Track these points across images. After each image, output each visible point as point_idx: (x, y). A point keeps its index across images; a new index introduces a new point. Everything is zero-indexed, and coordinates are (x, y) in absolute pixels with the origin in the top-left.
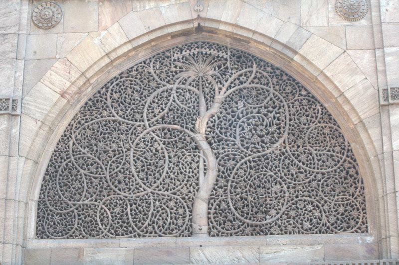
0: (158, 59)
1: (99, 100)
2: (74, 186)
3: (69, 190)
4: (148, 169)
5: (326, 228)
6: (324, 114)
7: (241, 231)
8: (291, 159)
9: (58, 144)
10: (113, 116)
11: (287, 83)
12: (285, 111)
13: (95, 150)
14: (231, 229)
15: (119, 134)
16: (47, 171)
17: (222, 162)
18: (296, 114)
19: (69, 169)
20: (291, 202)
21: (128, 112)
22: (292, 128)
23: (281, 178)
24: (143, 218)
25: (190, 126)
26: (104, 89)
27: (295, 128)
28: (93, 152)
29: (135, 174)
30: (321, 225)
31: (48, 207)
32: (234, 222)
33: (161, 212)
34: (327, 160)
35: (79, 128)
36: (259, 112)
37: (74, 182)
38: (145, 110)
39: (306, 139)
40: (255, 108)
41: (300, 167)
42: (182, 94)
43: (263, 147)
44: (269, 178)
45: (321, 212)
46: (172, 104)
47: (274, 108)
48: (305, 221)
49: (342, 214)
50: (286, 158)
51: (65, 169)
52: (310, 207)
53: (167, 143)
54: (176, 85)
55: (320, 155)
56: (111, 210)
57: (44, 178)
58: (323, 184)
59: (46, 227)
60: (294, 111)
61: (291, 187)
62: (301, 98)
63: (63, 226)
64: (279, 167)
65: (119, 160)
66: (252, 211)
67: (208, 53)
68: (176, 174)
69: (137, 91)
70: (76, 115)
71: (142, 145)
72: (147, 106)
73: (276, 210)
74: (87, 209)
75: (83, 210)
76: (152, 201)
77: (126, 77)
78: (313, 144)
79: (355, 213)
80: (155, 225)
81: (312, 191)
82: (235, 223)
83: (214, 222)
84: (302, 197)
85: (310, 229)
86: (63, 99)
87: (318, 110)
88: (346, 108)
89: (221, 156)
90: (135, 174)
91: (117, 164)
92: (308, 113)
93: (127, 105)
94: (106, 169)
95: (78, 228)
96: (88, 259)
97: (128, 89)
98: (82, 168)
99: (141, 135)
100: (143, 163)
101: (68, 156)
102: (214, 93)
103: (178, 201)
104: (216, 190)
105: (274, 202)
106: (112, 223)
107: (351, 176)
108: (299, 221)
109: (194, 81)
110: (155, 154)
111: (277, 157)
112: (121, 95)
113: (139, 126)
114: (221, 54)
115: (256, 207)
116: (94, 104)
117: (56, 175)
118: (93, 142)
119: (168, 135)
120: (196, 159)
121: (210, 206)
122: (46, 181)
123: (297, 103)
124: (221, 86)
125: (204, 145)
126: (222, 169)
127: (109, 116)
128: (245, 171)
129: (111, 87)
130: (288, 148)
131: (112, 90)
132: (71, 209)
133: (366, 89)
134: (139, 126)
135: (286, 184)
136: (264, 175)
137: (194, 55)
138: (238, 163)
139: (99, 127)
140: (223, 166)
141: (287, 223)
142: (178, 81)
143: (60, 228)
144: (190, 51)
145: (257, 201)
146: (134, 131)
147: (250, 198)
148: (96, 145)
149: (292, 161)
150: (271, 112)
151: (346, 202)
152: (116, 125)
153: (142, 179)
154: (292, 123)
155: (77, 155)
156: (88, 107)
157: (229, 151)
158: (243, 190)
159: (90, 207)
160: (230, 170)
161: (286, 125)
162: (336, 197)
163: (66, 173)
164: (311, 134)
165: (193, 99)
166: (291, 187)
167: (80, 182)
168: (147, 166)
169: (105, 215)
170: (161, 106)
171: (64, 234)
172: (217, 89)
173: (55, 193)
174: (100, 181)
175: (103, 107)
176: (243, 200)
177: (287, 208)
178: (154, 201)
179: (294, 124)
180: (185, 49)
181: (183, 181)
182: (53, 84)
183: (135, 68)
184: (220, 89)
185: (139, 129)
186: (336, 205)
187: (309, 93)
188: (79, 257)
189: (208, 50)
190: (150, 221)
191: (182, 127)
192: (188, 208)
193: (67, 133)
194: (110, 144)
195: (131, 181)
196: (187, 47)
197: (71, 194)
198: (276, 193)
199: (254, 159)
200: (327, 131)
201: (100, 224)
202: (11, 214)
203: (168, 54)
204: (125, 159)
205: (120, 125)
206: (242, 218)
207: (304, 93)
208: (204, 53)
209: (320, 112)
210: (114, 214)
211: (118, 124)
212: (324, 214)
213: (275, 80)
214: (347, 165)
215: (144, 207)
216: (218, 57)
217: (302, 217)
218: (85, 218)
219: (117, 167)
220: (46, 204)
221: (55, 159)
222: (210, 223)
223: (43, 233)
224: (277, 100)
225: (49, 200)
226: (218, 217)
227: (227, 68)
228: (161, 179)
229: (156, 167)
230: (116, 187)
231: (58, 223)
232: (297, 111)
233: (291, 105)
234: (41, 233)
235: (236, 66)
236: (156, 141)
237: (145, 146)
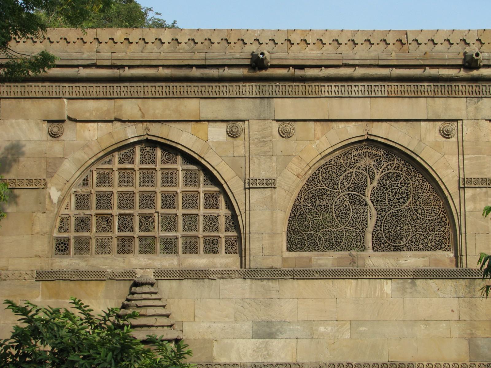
4: (342, 216)
10: (323, 186)
16: (290, 215)
17: (379, 213)
22: (414, 195)
23: (408, 221)
25: (362, 192)
26: (318, 171)
29: (336, 218)
36: (397, 186)
38: (339, 184)
39: (421, 201)
40: (395, 184)
43: (399, 205)
47: (405, 184)
49: (438, 241)
50: (411, 211)
51: (300, 215)
52: (422, 237)
54: (355, 170)
57: (289, 220)
65: (327, 210)
69: (335, 173)
76: (345, 232)
79: (444, 241)
82: (386, 245)
86: (298, 178)
89: (378, 209)
90: (336, 218)
96: (314, 263)
98: (308, 214)
99: (338, 197)
104: (376, 227)
105: (405, 234)
107: (443, 221)
109: (364, 168)
113: (337, 192)
116: (313, 180)
118: (313, 200)
119: (351, 198)
120: (366, 211)
123: (417, 182)
124: (378, 171)
125: (370, 203)
126: (379, 216)
128: (391, 218)
129: (321, 170)
130: (412, 206)
131: (322, 172)
133: (453, 177)
134: (337, 192)
136: (400, 220)
137: (364, 153)
140: (379, 215)
142: (356, 168)
143: (299, 246)
147: (393, 232)
148: (315, 202)
150: (404, 186)
153: (338, 221)
154: (414, 192)
162: (435, 232)
163: (300, 217)
165: (364, 178)
182: (293, 170)
183: (333, 160)
184: (378, 172)
185: (337, 194)
188: (310, 262)
189: (371, 150)
198: (406, 230)
200: (431, 197)
203: (350, 152)
206: (389, 242)
212: (429, 241)
213: (406, 168)
214: (441, 215)
216: (376, 155)
217: (418, 242)
223: (290, 248)
229: (346, 214)
230: (326, 224)
234: (289, 249)
236: (345, 200)
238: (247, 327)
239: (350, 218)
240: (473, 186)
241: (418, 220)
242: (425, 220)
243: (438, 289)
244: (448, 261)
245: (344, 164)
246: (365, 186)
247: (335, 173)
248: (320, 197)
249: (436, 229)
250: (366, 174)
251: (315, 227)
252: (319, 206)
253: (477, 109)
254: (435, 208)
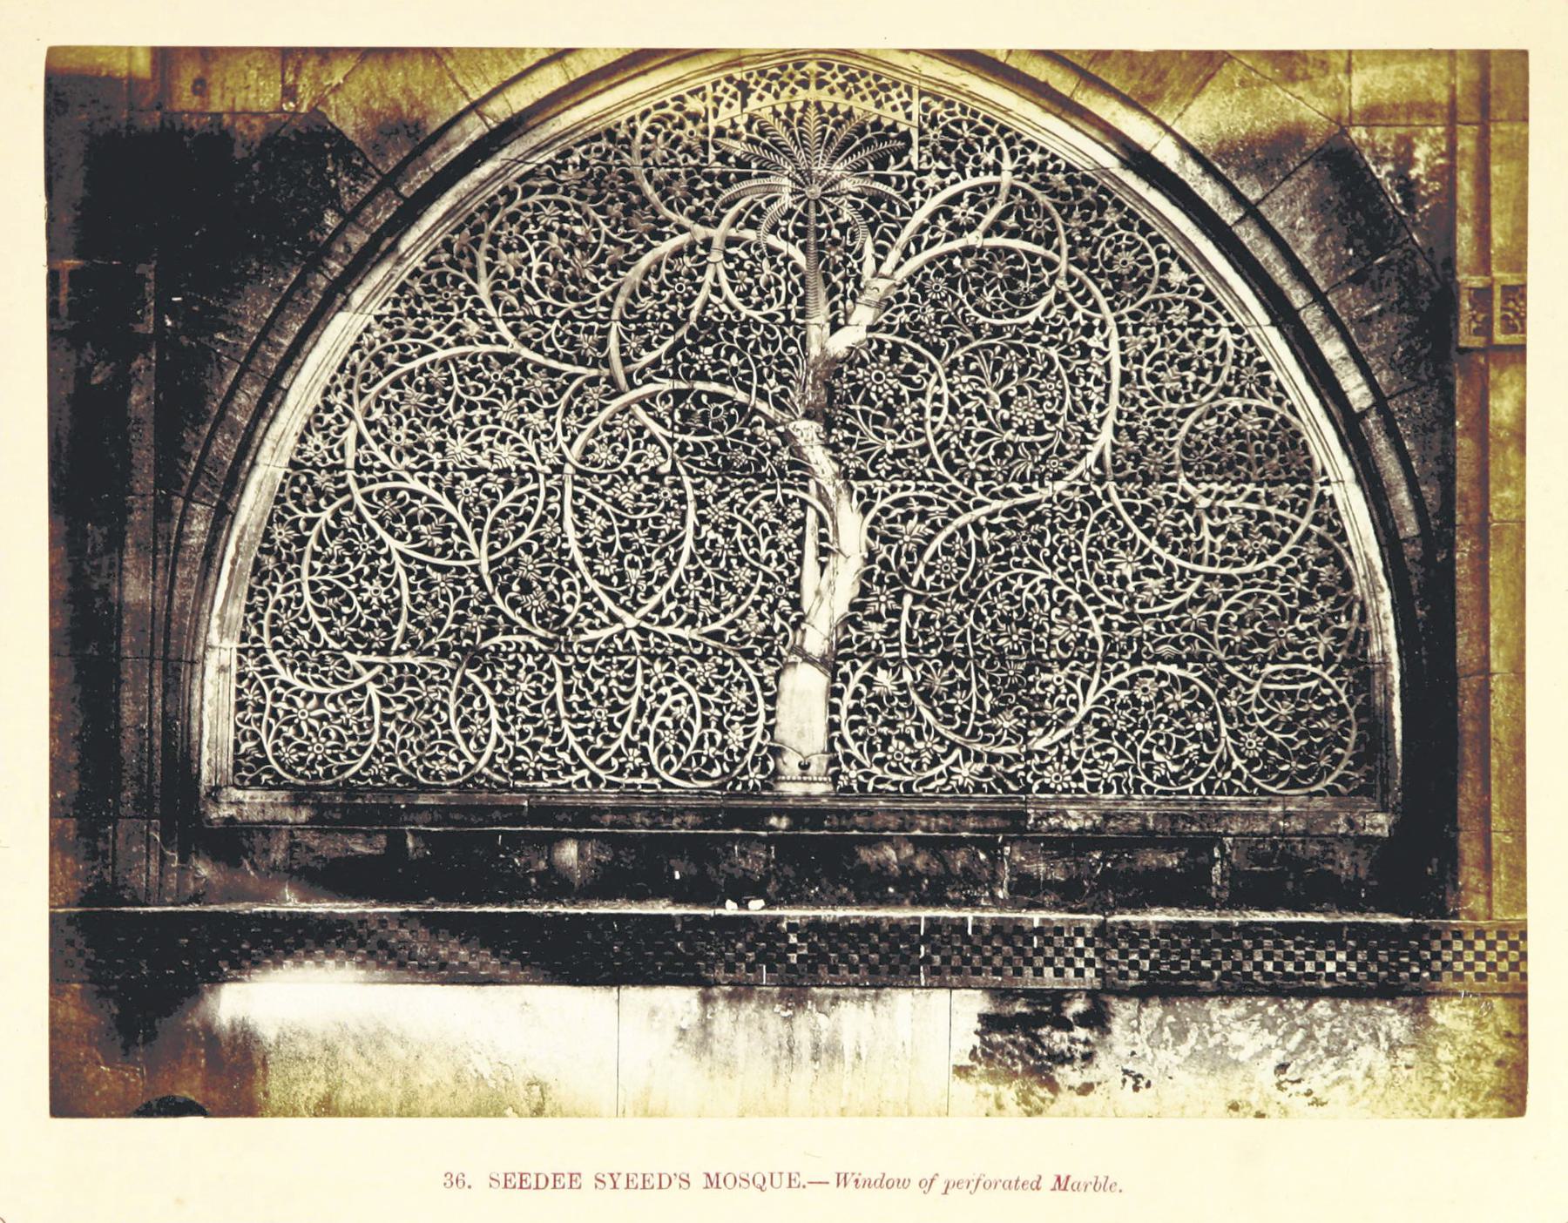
0: (658, 126)
1: (449, 279)
2: (365, 596)
3: (346, 610)
5: (1228, 775)
6: (1243, 363)
7: (941, 775)
8: (1119, 522)
9: (302, 440)
10: (501, 340)
11: (1119, 238)
12: (1106, 342)
13: (437, 466)
14: (908, 766)
15: (521, 410)
16: (267, 536)
17: (882, 529)
18: (1147, 359)
19: (347, 535)
20: (1114, 680)
21: (552, 327)
23: (1085, 590)
24: (610, 720)
27: (1141, 410)
28: (431, 475)
29: (580, 560)
30: (1213, 763)
31: (273, 671)
32: (919, 745)
33: (670, 699)
34: (1246, 528)
35: (378, 379)
37: (365, 584)
38: (616, 326)
39: (1176, 450)
41: (1152, 552)
42: (746, 265)
44: (1041, 588)
45: (1213, 716)
46: (709, 301)
48: (1160, 750)
50: (1102, 518)
51: (333, 534)
52: (1179, 700)
53: (690, 449)
56: (499, 688)
57: (258, 564)
58: (1225, 619)
59: (268, 747)
60: (1139, 347)
61: (1115, 625)
62: (1166, 295)
63: (329, 744)
64: (1079, 553)
66: (981, 705)
67: (842, 109)
68: (723, 564)
69: (583, 247)
70: (368, 330)
71: (604, 455)
72: (620, 301)
73: (1062, 704)
74: (413, 682)
75: (399, 683)
77: (545, 190)
78: (1198, 473)
80: (650, 745)
81: (1189, 640)
83: (850, 741)
84: (1153, 662)
85: (1175, 776)
87: (1224, 346)
89: (880, 504)
90: (580, 560)
91: (517, 520)
92: (1187, 355)
93: (548, 299)
94: (478, 537)
95: (382, 749)
97: (553, 235)
98: (391, 531)
99: (601, 417)
100: (609, 519)
101: (341, 486)
102: (860, 265)
103: (730, 663)
104: (859, 626)
106: (502, 734)
108: (1140, 748)
109: (790, 213)
111: (1071, 515)
112: (528, 260)
115: (996, 693)
117: (301, 555)
118: (431, 435)
121: (839, 685)
122: (265, 575)
127: (486, 340)
128: (963, 562)
130: (1111, 486)
131: (494, 239)
132: (357, 682)
134: (593, 382)
135: (1098, 613)
136: (1027, 578)
138: (938, 529)
139: (450, 381)
140: (884, 540)
141: (1097, 755)
142: (731, 213)
144: (777, 95)
145: (1000, 671)
146: (577, 402)
148: (440, 447)
149: (1123, 533)
151: (1303, 686)
152: (511, 374)
155: (372, 481)
156: (407, 301)
157: (906, 488)
158: (952, 629)
159: (423, 674)
160: (909, 556)
161: (1107, 399)
163: (335, 547)
164: (1193, 436)
166: (1115, 625)
167: (385, 582)
168: (622, 530)
169: (477, 703)
170: (672, 307)
171: (334, 772)
173: (296, 621)
174: (457, 582)
175: (461, 303)
176: (952, 666)
177: (1101, 701)
178: (647, 661)
179: (1137, 395)
180: (759, 90)
181: (747, 590)
186: (1265, 693)
187: (1197, 280)
189: (839, 97)
190: (634, 731)
191: (747, 389)
192: (764, 688)
193: (331, 398)
194: (490, 444)
195: (564, 583)
196: (764, 82)
197: (356, 624)
199: (995, 521)
201: (459, 738)
203: (693, 105)
204: (546, 504)
205: (525, 374)
207: (1177, 276)
208: (827, 107)
209: (1231, 355)
210: (507, 704)
211: (518, 373)
212: (1224, 726)
215: (613, 683)
216: (877, 125)
218: (407, 713)
219: (518, 532)
220: (265, 661)
221: (293, 496)
222: (837, 746)
224: (1082, 300)
225: (276, 646)
226: (863, 723)
228: (671, 584)
229: (654, 535)
230: (514, 604)
231: (311, 728)
232: (1150, 347)
233: (1127, 320)
235: (941, 165)
236: (652, 440)
237: (615, 459)
241: (1150, 582)
242: (1198, 581)
245: (649, 189)
246: (789, 343)
247: (583, 246)
248: (478, 413)
249: (1273, 646)
250: (800, 259)
251: (439, 623)
252: (472, 474)
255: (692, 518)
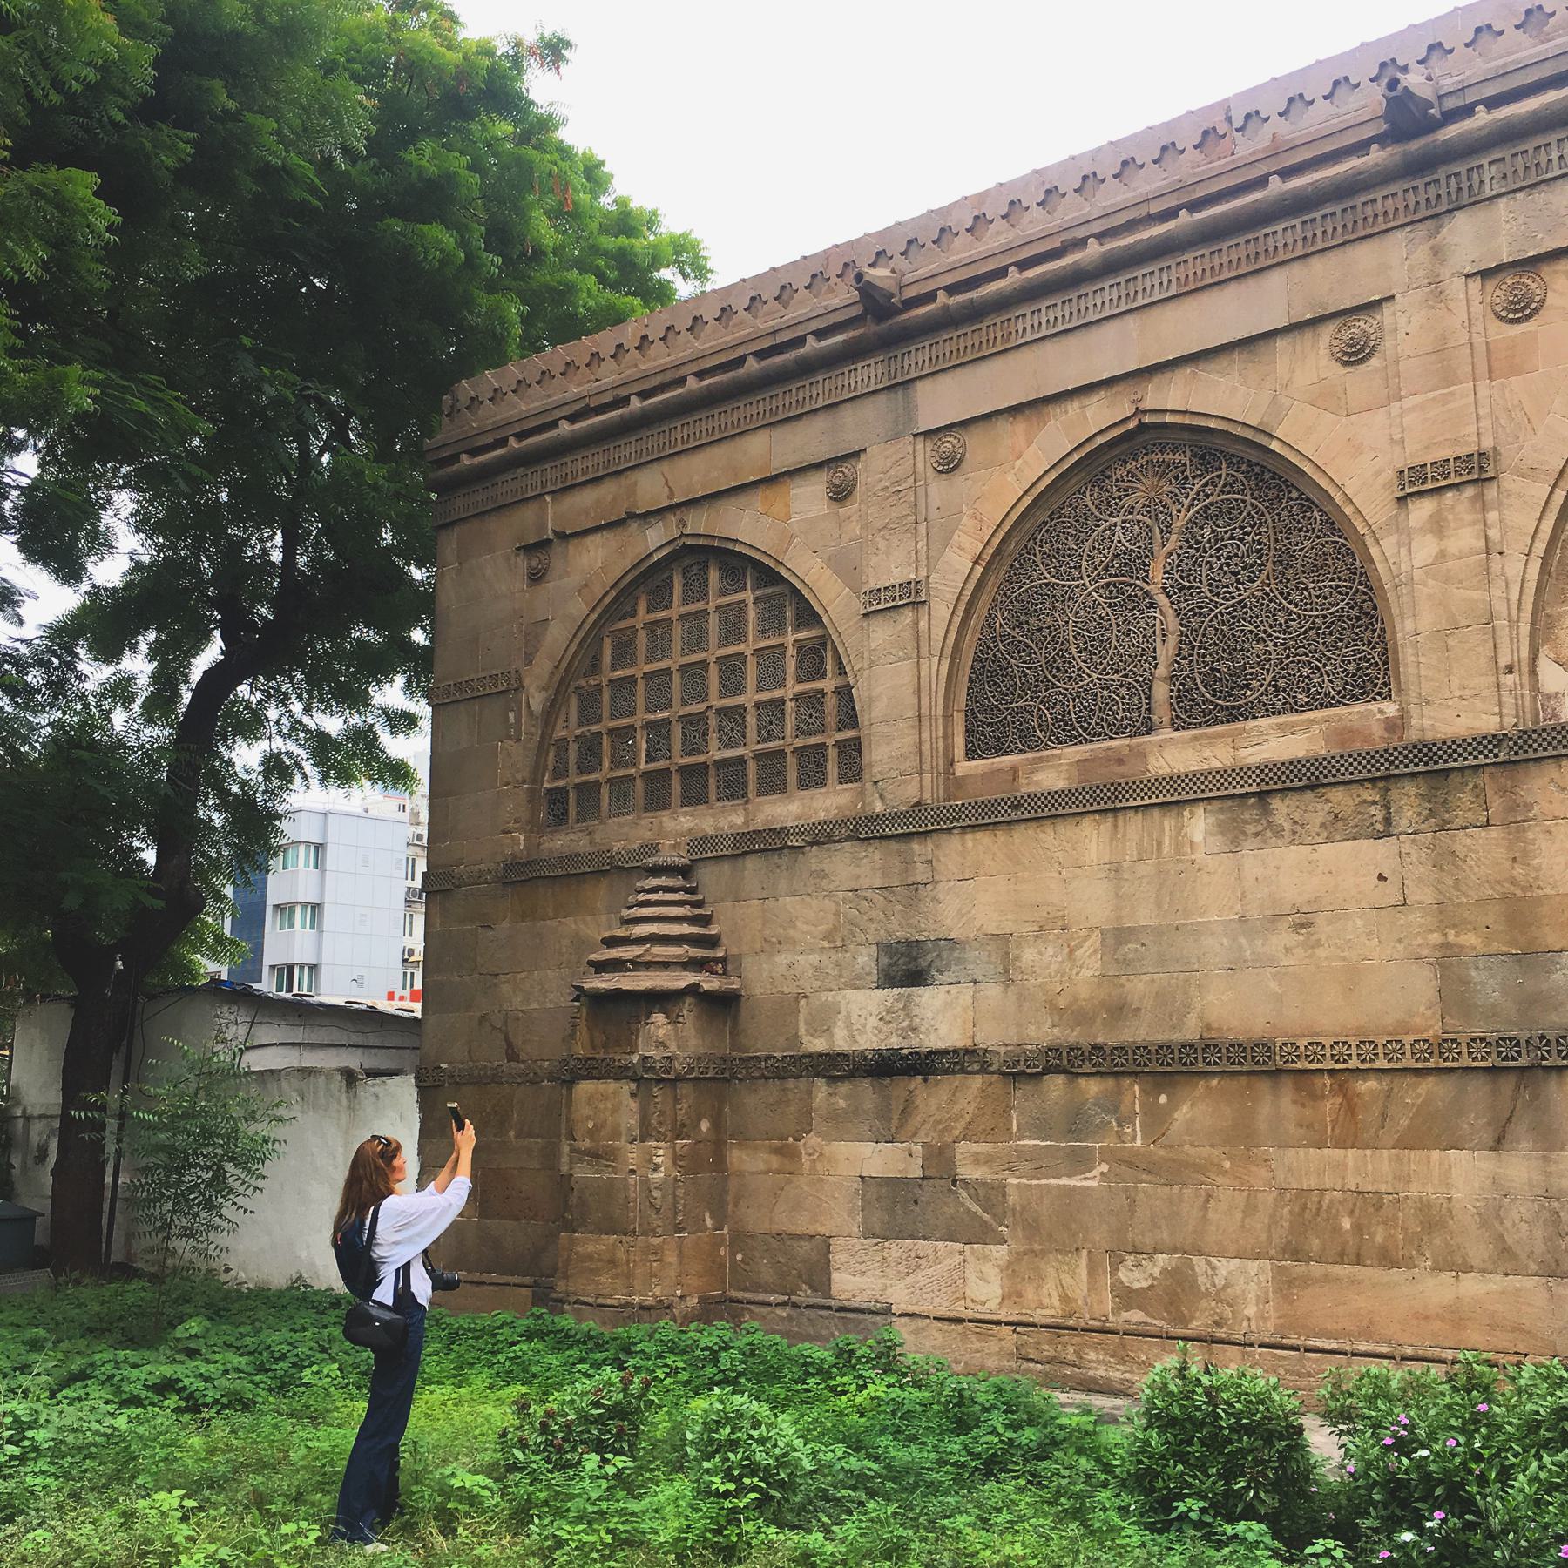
4: (1092, 646)
23: (1265, 631)
29: (1076, 655)
36: (1232, 538)
38: (1084, 562)
40: (1226, 532)
43: (1239, 590)
45: (1322, 675)
47: (1253, 527)
49: (1354, 675)
50: (1271, 601)
52: (1306, 671)
55: (1320, 589)
85: (1307, 703)
88: (1348, 510)
104: (1178, 663)
107: (1367, 614)
110: (1099, 624)
114: (1177, 458)
125: (1162, 600)
130: (1273, 586)
134: (1077, 586)
140: (1186, 626)
143: (992, 742)
148: (1027, 622)
150: (1248, 534)
153: (1085, 662)
172: (1174, 513)
184: (1179, 511)
198: (1258, 657)
202: (926, 736)
207: (1295, 495)
227: (1186, 478)
229: (1102, 641)
230: (1054, 677)
234: (971, 754)
238: (866, 959)
239: (1111, 651)
240: (1429, 486)
243: (1336, 816)
244: (1378, 731)
245: (1092, 508)
246: (1147, 556)
253: (1436, 252)
254: (1340, 579)
255: (1115, 632)
